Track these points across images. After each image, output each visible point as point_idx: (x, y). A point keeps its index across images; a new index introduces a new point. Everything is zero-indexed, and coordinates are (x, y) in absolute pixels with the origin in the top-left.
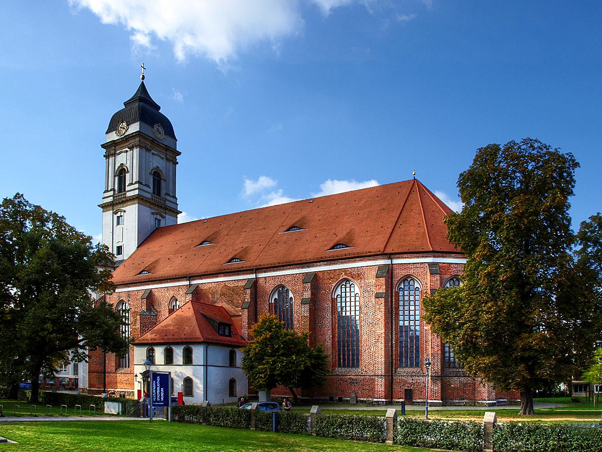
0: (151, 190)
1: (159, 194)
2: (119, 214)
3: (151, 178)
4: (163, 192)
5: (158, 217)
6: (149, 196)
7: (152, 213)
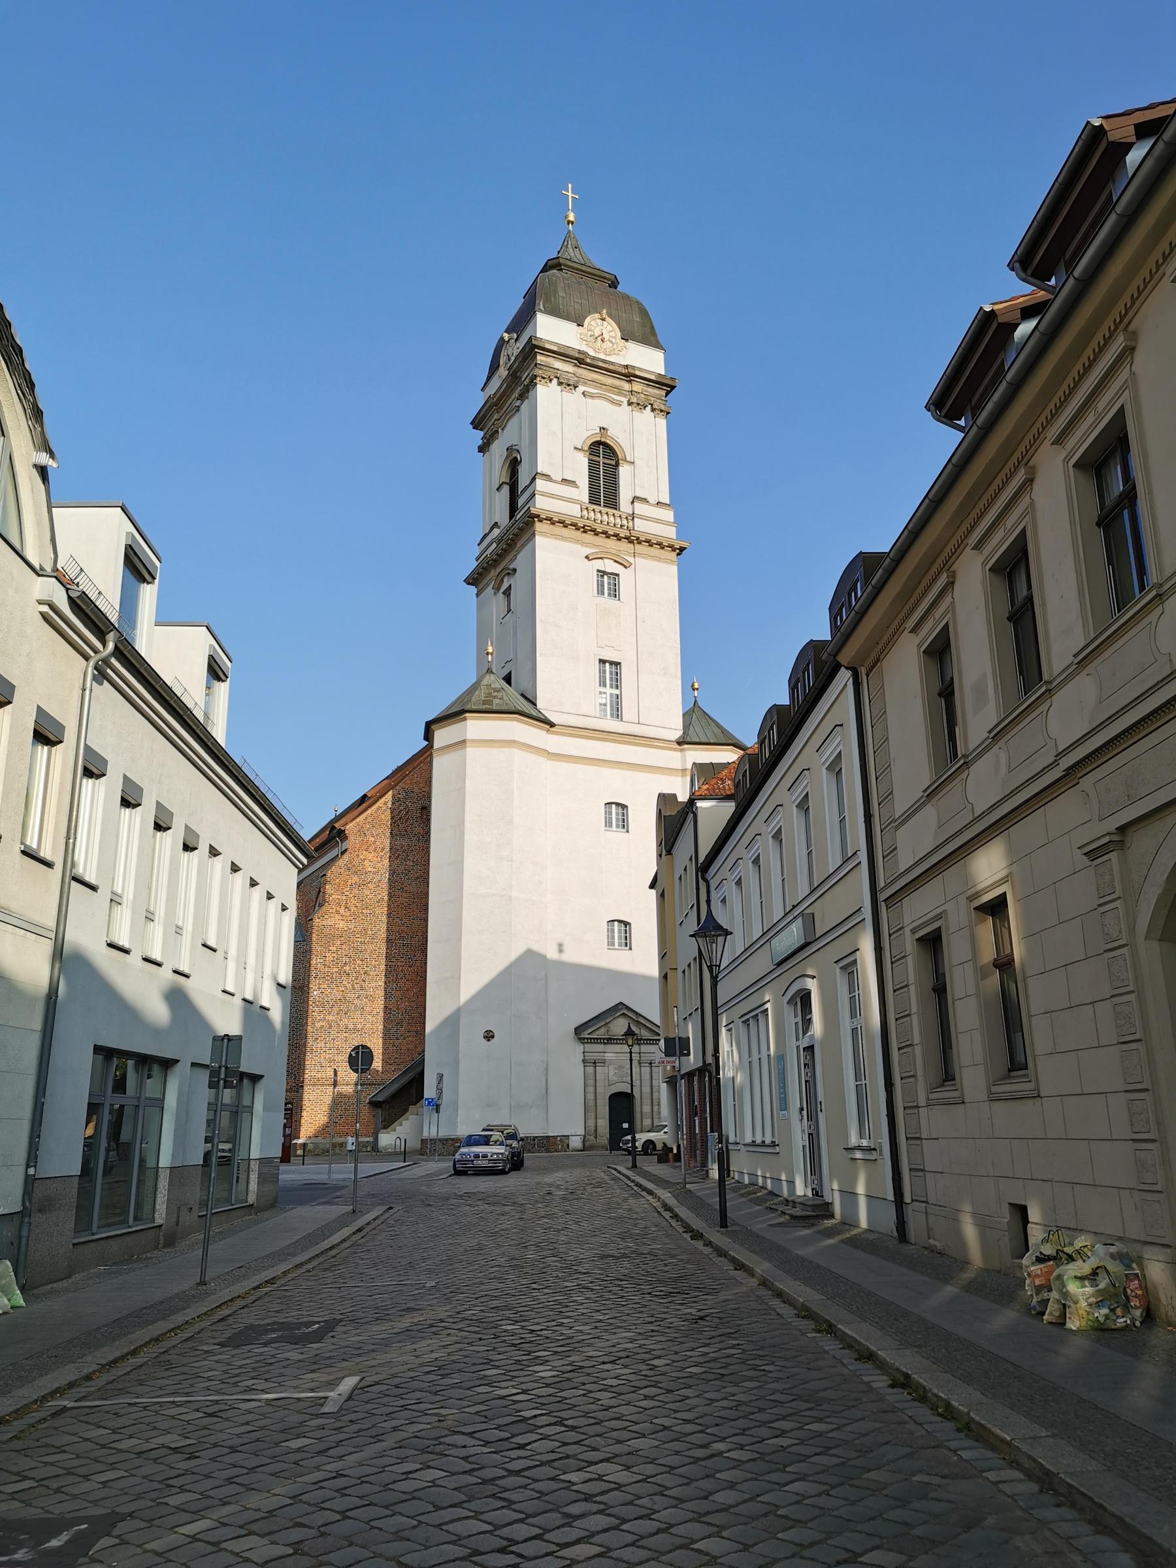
0: (583, 494)
1: (612, 502)
2: (505, 586)
3: (583, 461)
4: (625, 496)
5: (611, 567)
6: (573, 511)
7: (587, 557)
